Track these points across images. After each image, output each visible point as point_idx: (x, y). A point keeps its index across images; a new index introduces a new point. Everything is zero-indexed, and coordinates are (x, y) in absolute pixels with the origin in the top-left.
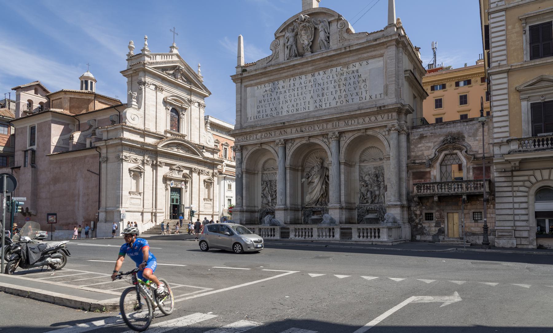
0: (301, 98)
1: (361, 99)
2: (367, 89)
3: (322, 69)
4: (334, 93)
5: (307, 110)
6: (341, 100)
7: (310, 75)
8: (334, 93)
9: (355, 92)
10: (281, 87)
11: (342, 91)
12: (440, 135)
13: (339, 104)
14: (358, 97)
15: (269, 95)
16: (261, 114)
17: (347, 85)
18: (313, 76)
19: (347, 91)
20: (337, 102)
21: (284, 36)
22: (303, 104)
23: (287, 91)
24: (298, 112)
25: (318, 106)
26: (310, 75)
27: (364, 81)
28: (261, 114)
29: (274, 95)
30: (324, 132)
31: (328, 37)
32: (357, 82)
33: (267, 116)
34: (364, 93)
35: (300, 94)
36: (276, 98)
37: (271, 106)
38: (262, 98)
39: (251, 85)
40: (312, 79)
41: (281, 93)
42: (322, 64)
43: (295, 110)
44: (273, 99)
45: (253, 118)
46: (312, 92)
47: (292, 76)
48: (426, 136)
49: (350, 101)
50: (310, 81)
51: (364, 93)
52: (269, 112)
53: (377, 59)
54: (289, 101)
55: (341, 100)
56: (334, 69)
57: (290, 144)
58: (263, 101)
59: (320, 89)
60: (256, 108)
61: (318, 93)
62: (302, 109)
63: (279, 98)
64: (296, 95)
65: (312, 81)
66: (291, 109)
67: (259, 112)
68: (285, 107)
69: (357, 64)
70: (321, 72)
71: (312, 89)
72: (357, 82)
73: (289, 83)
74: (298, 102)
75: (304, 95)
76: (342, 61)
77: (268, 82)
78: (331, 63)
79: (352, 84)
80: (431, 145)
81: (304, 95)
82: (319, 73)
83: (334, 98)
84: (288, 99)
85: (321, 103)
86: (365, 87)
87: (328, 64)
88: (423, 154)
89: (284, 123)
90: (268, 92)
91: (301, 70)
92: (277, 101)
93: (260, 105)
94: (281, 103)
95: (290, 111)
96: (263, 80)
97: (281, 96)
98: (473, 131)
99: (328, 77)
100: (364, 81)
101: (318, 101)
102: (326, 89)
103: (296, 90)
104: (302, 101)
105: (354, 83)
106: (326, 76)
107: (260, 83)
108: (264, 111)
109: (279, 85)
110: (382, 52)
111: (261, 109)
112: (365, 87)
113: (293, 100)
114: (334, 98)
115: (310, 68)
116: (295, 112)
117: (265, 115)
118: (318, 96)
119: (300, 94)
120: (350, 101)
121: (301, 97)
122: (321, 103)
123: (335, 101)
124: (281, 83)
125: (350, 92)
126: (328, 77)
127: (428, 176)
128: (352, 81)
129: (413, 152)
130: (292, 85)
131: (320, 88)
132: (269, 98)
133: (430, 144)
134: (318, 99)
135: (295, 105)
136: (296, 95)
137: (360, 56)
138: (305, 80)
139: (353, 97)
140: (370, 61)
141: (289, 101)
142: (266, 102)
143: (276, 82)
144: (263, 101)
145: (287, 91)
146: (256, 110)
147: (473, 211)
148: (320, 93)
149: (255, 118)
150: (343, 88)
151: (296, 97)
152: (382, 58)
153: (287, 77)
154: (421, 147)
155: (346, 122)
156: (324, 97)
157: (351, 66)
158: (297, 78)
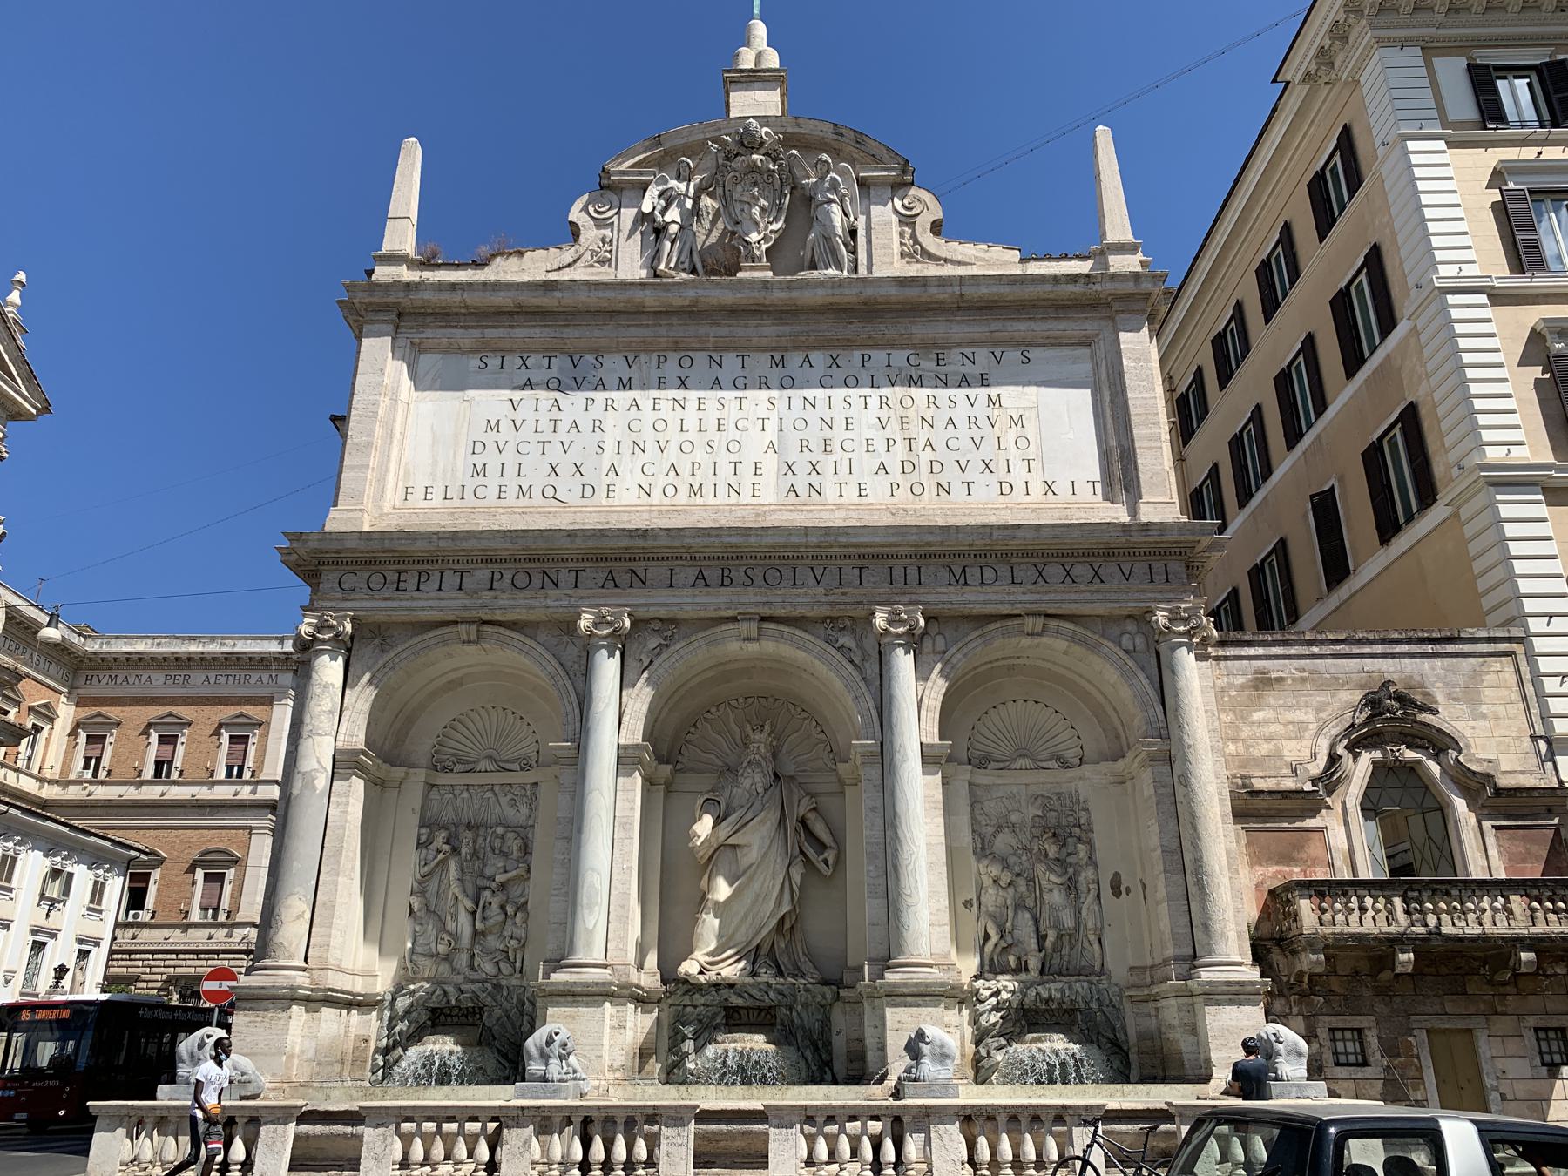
2: (1032, 452)
3: (821, 345)
4: (879, 445)
5: (746, 498)
6: (914, 478)
7: (765, 358)
8: (879, 445)
9: (976, 457)
12: (1336, 683)
13: (903, 494)
14: (993, 480)
16: (493, 482)
17: (940, 424)
19: (939, 445)
20: (894, 487)
21: (644, 187)
22: (726, 470)
24: (698, 501)
25: (802, 489)
26: (765, 358)
28: (493, 482)
31: (853, 233)
34: (1019, 470)
37: (554, 454)
39: (446, 350)
42: (827, 327)
43: (684, 490)
44: (563, 426)
46: (772, 426)
48: (1280, 680)
51: (1019, 470)
52: (537, 477)
53: (1066, 351)
54: (651, 447)
55: (914, 478)
56: (879, 356)
57: (653, 642)
58: (506, 426)
59: (814, 422)
60: (464, 449)
61: (801, 435)
63: (597, 426)
66: (662, 480)
67: (479, 471)
69: (982, 355)
70: (818, 357)
71: (774, 417)
73: (659, 373)
74: (699, 455)
75: (733, 433)
77: (549, 351)
79: (962, 423)
80: (1308, 716)
81: (733, 433)
84: (649, 437)
85: (815, 480)
86: (1022, 443)
88: (1278, 755)
91: (723, 331)
92: (588, 438)
93: (490, 438)
94: (610, 446)
96: (519, 333)
97: (610, 420)
98: (1460, 680)
100: (1017, 422)
101: (802, 468)
102: (839, 424)
104: (724, 460)
107: (502, 350)
109: (601, 373)
111: (492, 459)
112: (1022, 443)
113: (673, 449)
116: (682, 498)
118: (804, 446)
120: (958, 492)
122: (815, 480)
123: (883, 482)
127: (1314, 848)
128: (961, 412)
129: (1235, 740)
131: (813, 416)
132: (544, 418)
133: (1299, 715)
134: (802, 463)
135: (685, 470)
139: (967, 477)
140: (1034, 353)
141: (651, 447)
142: (527, 431)
143: (590, 358)
144: (506, 426)
146: (463, 462)
147: (1532, 1021)
148: (814, 435)
149: (454, 492)
152: (1087, 351)
153: (647, 348)
154: (1266, 722)
155: (957, 570)
157: (955, 356)
158: (701, 358)
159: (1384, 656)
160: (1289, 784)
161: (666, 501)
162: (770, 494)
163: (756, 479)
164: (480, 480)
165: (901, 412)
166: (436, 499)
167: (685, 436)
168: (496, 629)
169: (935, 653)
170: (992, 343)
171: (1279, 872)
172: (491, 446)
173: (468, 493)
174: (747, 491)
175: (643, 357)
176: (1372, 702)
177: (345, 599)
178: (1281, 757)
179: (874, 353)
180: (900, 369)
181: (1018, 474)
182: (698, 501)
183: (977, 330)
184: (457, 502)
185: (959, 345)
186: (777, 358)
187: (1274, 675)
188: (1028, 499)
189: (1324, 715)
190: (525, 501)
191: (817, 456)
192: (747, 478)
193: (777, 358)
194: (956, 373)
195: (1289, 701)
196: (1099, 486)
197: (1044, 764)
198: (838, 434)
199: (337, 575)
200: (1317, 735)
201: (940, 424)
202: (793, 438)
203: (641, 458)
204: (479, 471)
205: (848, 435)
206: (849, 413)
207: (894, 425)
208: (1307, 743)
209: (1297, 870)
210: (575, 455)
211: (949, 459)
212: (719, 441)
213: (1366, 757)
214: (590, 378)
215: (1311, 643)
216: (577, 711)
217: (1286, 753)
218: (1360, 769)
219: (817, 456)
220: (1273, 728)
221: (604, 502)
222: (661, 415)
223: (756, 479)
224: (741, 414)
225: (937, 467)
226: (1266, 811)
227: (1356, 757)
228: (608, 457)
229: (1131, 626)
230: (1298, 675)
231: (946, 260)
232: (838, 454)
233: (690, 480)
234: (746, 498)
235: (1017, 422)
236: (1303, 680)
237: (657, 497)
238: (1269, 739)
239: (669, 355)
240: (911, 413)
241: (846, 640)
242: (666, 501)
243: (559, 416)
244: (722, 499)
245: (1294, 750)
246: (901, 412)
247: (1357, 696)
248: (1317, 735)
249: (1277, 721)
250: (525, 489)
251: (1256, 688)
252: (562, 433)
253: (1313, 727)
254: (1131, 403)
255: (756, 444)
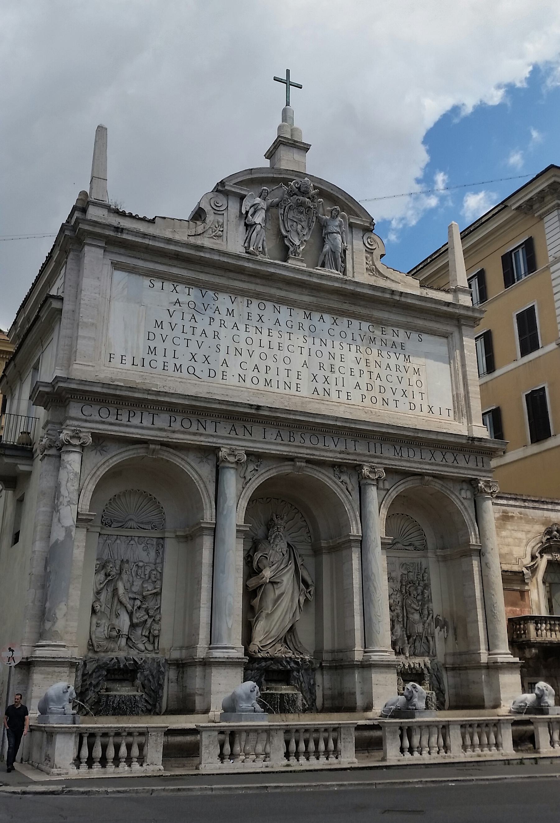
0: (280, 357)
1: (412, 406)
2: (423, 390)
4: (356, 373)
5: (293, 391)
7: (301, 312)
8: (356, 373)
10: (224, 311)
11: (374, 376)
12: (532, 521)
14: (407, 401)
15: (188, 317)
16: (160, 359)
18: (309, 317)
19: (383, 378)
20: (363, 397)
23: (242, 327)
27: (417, 372)
28: (160, 359)
29: (202, 322)
30: (350, 459)
31: (345, 251)
32: (402, 369)
33: (178, 368)
34: (418, 397)
35: (275, 345)
36: (210, 334)
38: (165, 318)
40: (306, 323)
41: (222, 324)
43: (262, 382)
44: (198, 331)
45: (128, 360)
46: (305, 352)
47: (258, 296)
48: (512, 517)
49: (392, 403)
50: (301, 327)
51: (418, 397)
52: (185, 361)
53: (437, 339)
54: (245, 353)
55: (372, 393)
56: (356, 323)
59: (326, 354)
61: (320, 360)
62: (282, 385)
63: (216, 335)
64: (265, 343)
65: (306, 327)
67: (152, 351)
68: (234, 361)
69: (402, 332)
70: (326, 317)
71: (306, 346)
72: (402, 369)
74: (270, 362)
76: (377, 314)
78: (353, 308)
79: (393, 368)
82: (322, 317)
83: (358, 385)
84: (243, 345)
85: (326, 386)
87: (346, 307)
88: (511, 553)
89: (258, 408)
90: (185, 307)
91: (283, 294)
92: (210, 341)
93: (158, 331)
94: (223, 349)
95: (248, 380)
97: (223, 332)
99: (343, 334)
102: (338, 357)
103: (265, 332)
104: (282, 367)
105: (397, 368)
106: (337, 329)
108: (170, 354)
109: (217, 303)
110: (449, 329)
113: (256, 355)
114: (358, 385)
115: (306, 299)
117: (171, 367)
118: (321, 367)
119: (275, 345)
120: (392, 403)
121: (280, 355)
122: (326, 386)
124: (224, 301)
125: (391, 385)
126: (343, 334)
130: (255, 317)
133: (520, 535)
135: (263, 369)
136: (265, 343)
137: (409, 319)
138: (289, 318)
140: (424, 336)
141: (245, 353)
143: (211, 293)
145: (242, 327)
146: (142, 343)
150: (376, 371)
151: (266, 350)
152: (445, 340)
153: (242, 293)
156: (334, 376)
157: (389, 330)
158: (269, 305)
159: (552, 510)
160: (516, 568)
161: (253, 386)
162: (305, 392)
163: (298, 381)
164: (152, 356)
165: (366, 356)
166: (128, 365)
167: (262, 350)
168: (168, 449)
169: (385, 490)
170: (408, 327)
171: (511, 610)
172: (158, 337)
173: (146, 363)
174: (294, 387)
175: (239, 299)
176: (549, 532)
177: (86, 421)
178: (512, 554)
179: (353, 320)
180: (366, 333)
181: (417, 400)
182: (268, 388)
183: (402, 319)
184: (140, 368)
185: (392, 326)
186: (308, 313)
187: (510, 514)
188: (421, 414)
189: (529, 536)
190: (178, 374)
191: (328, 373)
192: (294, 381)
193: (308, 313)
194: (390, 340)
195: (516, 528)
196: (452, 413)
197: (407, 548)
198: (337, 363)
199: (81, 405)
200: (527, 545)
201: (384, 366)
202: (315, 361)
203: (240, 359)
204: (152, 351)
205: (342, 364)
206: (342, 352)
207: (363, 362)
208: (522, 549)
209: (518, 609)
210: (204, 350)
211: (388, 386)
212: (280, 355)
213: (546, 557)
214: (211, 305)
215: (525, 501)
216: (213, 503)
217: (514, 553)
218: (543, 563)
219: (328, 373)
220: (510, 540)
221: (221, 381)
222: (250, 335)
223: (298, 381)
224: (290, 342)
225: (382, 389)
226: (515, 580)
227: (542, 556)
228: (222, 355)
229: (465, 486)
230: (520, 515)
231: (387, 277)
232: (337, 374)
233: (266, 376)
234: (293, 391)
235: (417, 372)
236: (521, 518)
237: (248, 383)
238: (508, 545)
239: (254, 301)
240: (370, 358)
241: (344, 478)
242: (253, 386)
243: (195, 325)
244: (281, 390)
245: (518, 551)
246: (366, 356)
247: (543, 529)
248: (527, 545)
249: (511, 537)
250: (178, 366)
251: (503, 520)
252: (197, 337)
253: (525, 542)
254: (468, 373)
255: (298, 361)
